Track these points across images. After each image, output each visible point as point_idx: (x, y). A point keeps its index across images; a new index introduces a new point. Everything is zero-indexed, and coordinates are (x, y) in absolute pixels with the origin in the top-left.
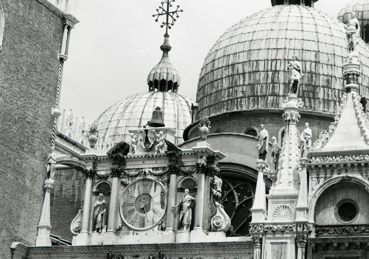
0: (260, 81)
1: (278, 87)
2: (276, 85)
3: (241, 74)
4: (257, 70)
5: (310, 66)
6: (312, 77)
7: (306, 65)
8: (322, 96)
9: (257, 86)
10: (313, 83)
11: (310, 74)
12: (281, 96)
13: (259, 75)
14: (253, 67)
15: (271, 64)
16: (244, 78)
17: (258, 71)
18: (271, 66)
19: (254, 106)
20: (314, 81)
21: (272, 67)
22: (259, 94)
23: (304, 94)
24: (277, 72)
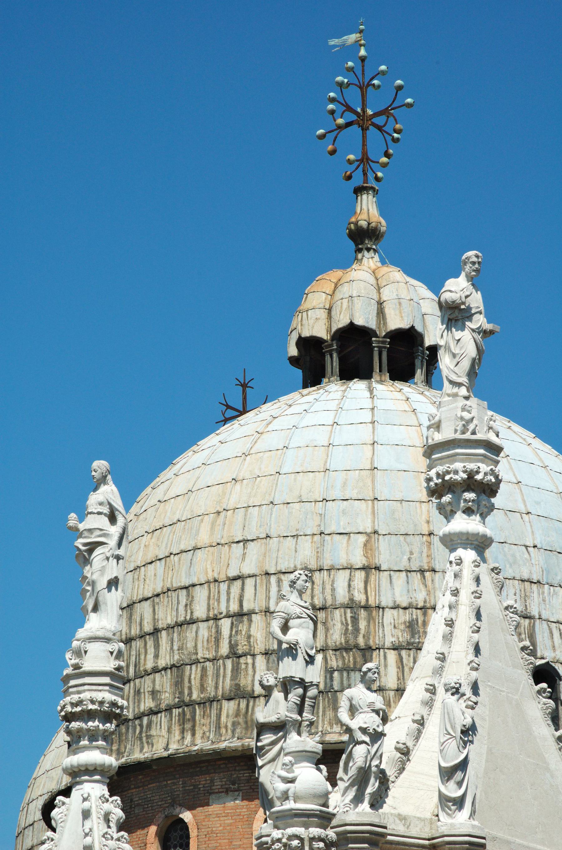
0: (197, 654)
1: (250, 666)
2: (242, 660)
3: (149, 634)
4: (188, 618)
5: (349, 586)
6: (355, 620)
7: (333, 582)
8: (395, 678)
9: (191, 669)
10: (361, 641)
11: (349, 611)
12: (259, 696)
13: (194, 634)
14: (177, 609)
15: (228, 593)
16: (157, 646)
17: (193, 622)
18: (228, 600)
19: (183, 738)
20: (362, 631)
21: (231, 603)
22: (195, 696)
23: (332, 679)
24: (245, 618)
